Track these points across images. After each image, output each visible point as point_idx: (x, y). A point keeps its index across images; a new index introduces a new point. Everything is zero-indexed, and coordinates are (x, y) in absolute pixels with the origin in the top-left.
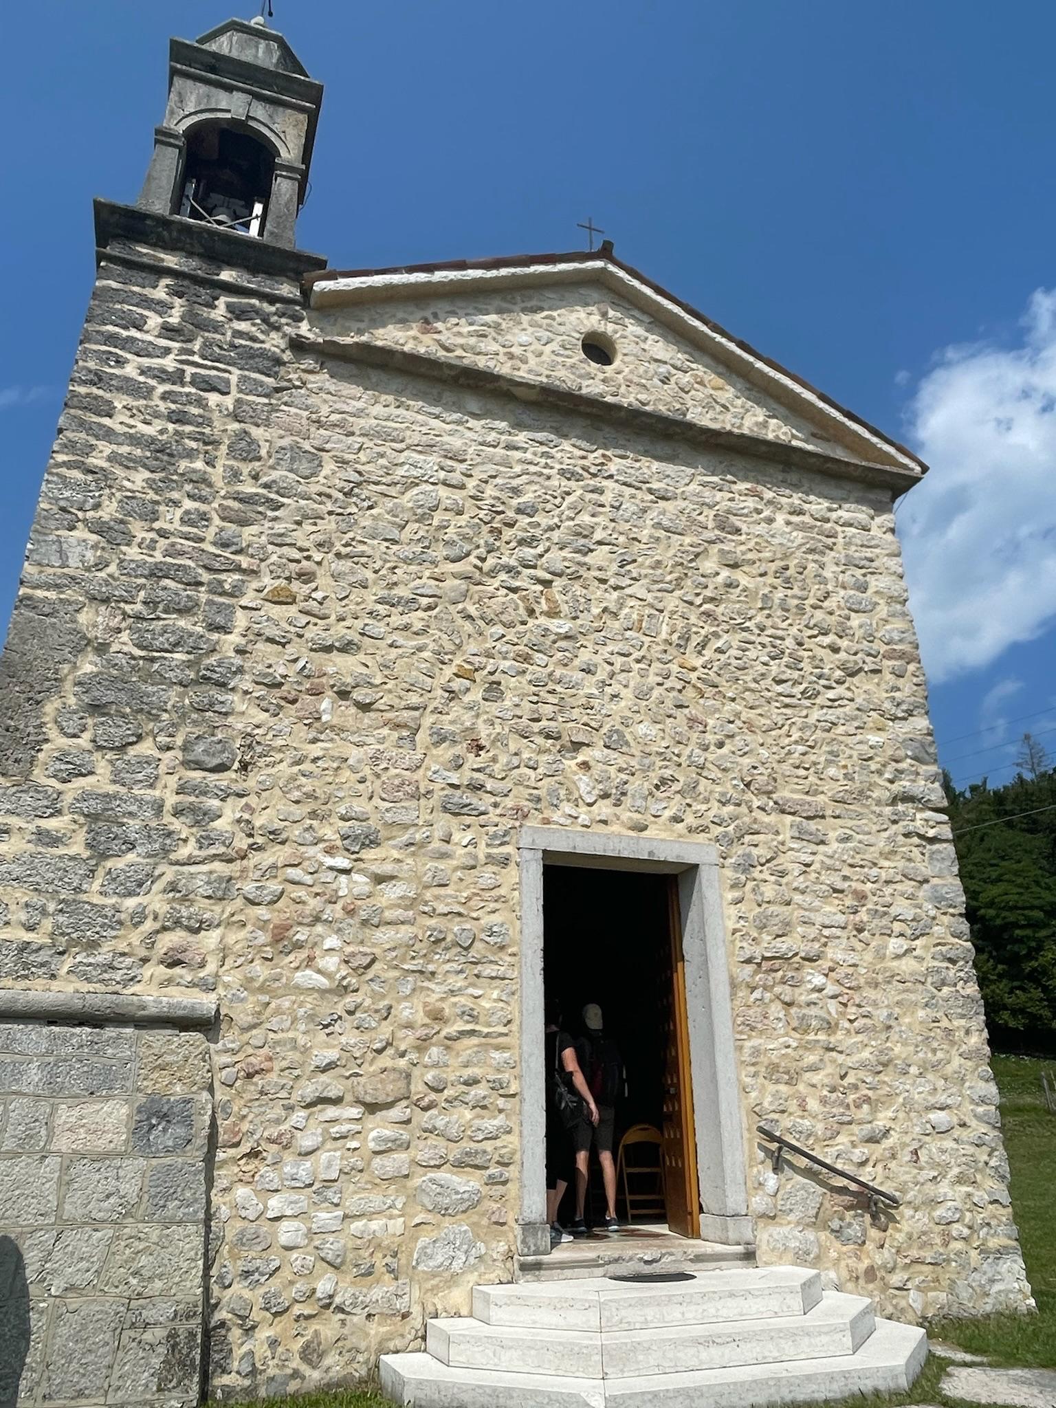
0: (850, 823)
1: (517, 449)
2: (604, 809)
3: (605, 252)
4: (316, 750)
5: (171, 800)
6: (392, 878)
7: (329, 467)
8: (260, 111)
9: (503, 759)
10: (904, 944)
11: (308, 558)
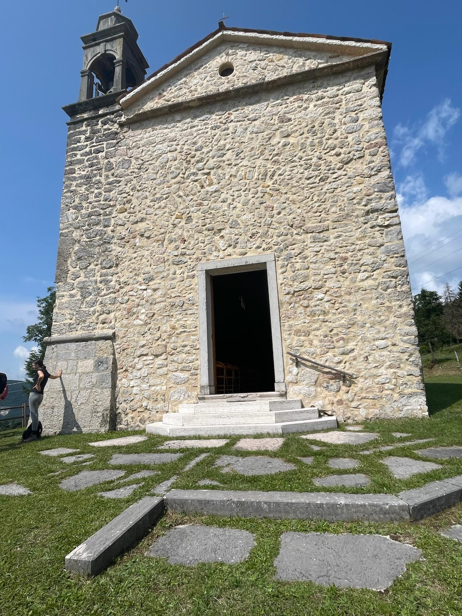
0: (340, 229)
1: (194, 127)
2: (230, 250)
3: (222, 27)
5: (99, 279)
6: (158, 289)
7: (133, 161)
9: (192, 242)
10: (367, 274)
11: (129, 195)
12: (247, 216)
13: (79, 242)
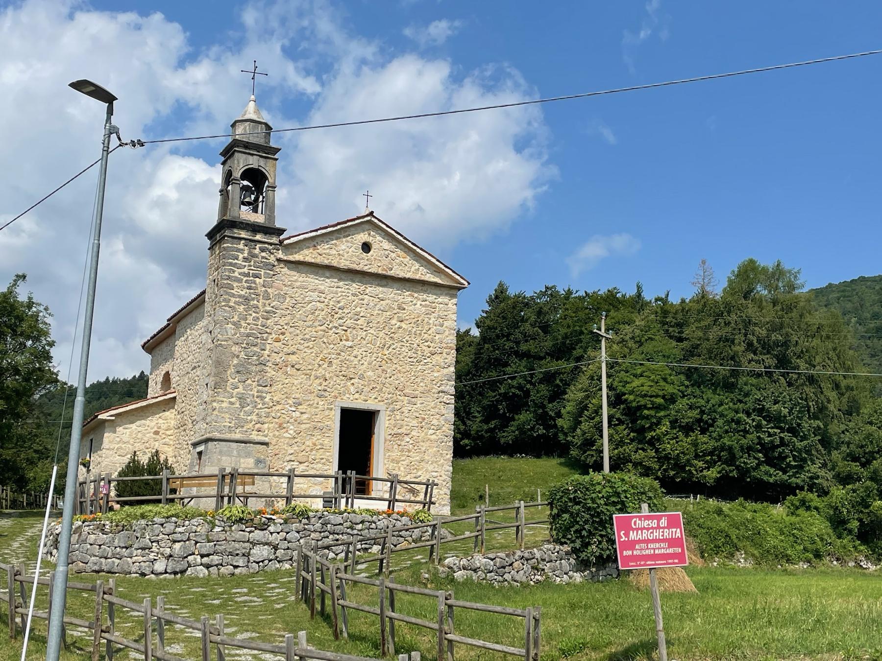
2: (357, 396)
4: (287, 381)
5: (256, 394)
7: (288, 299)
8: (262, 162)
12: (370, 373)
13: (238, 357)
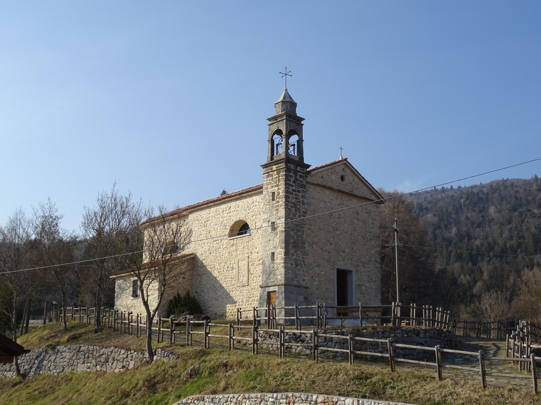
13: (293, 238)
